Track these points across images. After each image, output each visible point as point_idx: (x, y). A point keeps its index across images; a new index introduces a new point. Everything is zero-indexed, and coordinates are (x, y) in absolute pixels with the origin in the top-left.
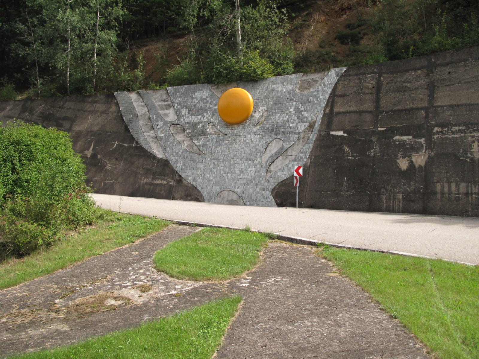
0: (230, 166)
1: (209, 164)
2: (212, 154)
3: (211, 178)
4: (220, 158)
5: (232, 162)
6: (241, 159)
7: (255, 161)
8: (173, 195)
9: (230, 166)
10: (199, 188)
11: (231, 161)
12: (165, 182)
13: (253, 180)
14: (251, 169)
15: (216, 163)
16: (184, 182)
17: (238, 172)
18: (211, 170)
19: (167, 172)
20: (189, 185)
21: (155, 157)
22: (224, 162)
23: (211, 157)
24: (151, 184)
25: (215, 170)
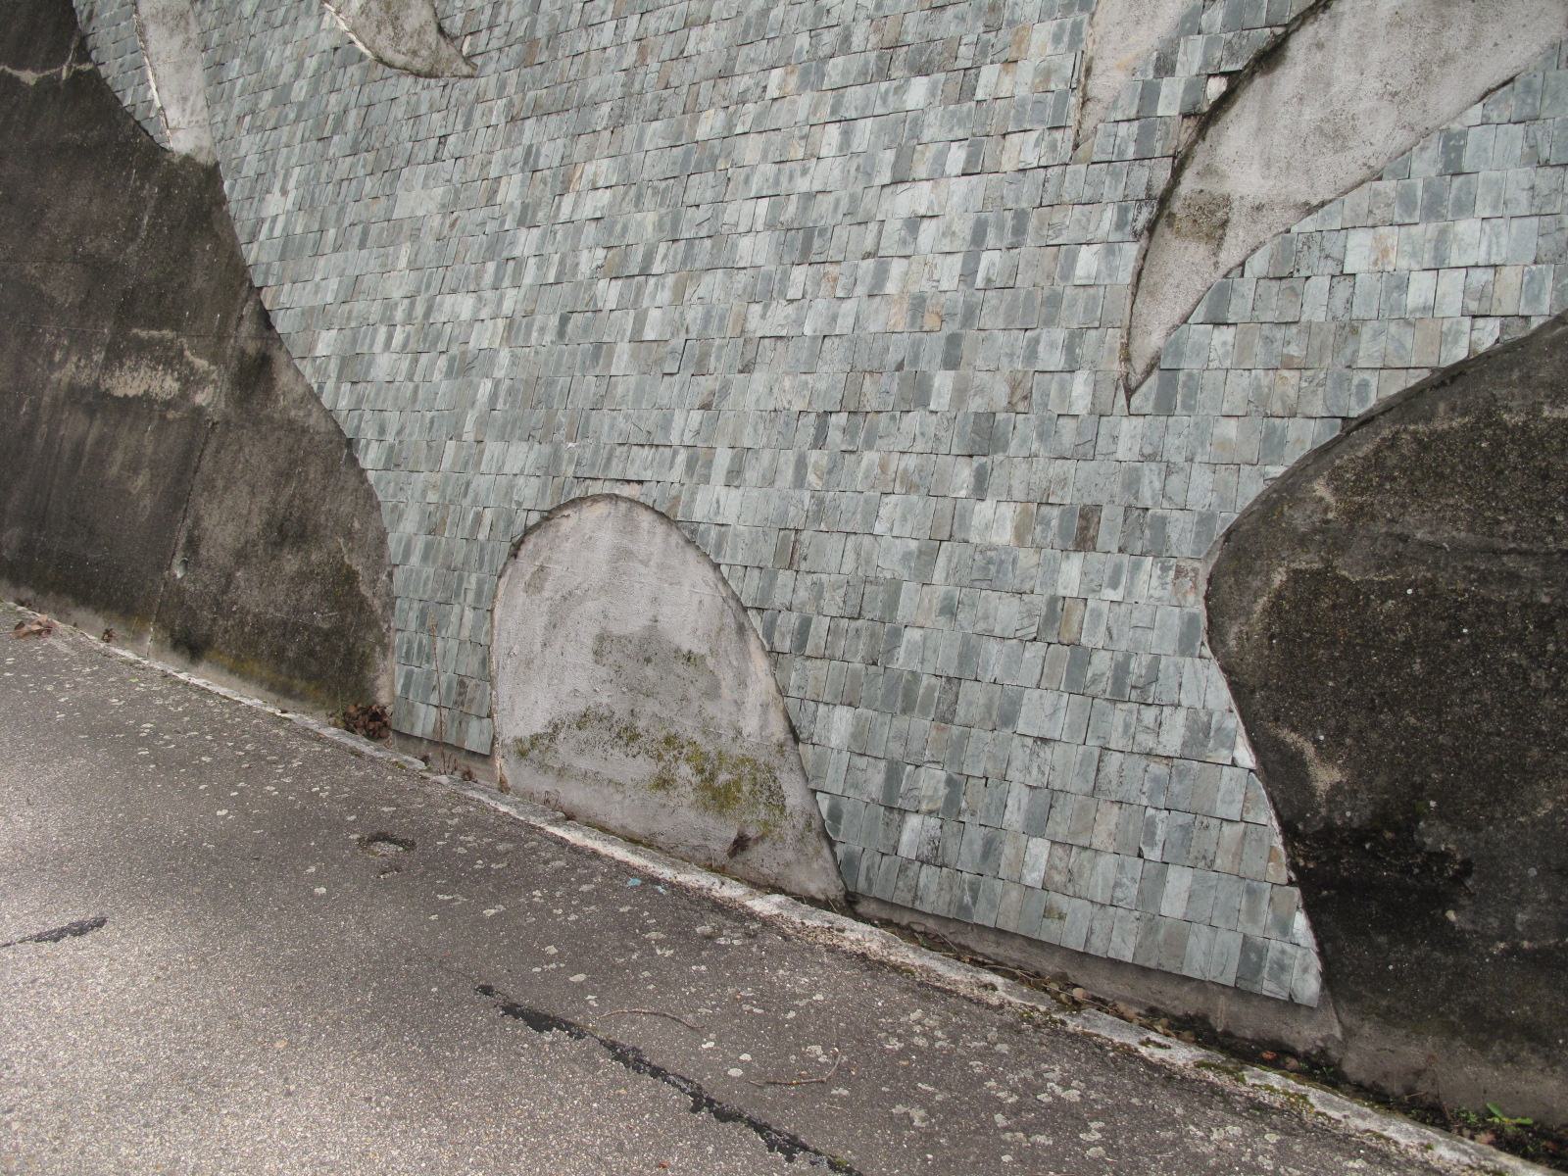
0: (683, 174)
1: (494, 172)
2: (529, 54)
3: (484, 337)
4: (594, 85)
5: (710, 124)
6: (811, 73)
7: (989, 74)
8: (198, 520)
9: (683, 174)
10: (370, 458)
11: (693, 111)
12: (170, 385)
13: (934, 347)
14: (916, 198)
15: (550, 154)
16: (284, 378)
17: (754, 249)
18: (496, 246)
19: (199, 282)
20: (315, 420)
21: (154, 153)
22: (630, 131)
23: (522, 88)
24: (97, 402)
25: (526, 242)
